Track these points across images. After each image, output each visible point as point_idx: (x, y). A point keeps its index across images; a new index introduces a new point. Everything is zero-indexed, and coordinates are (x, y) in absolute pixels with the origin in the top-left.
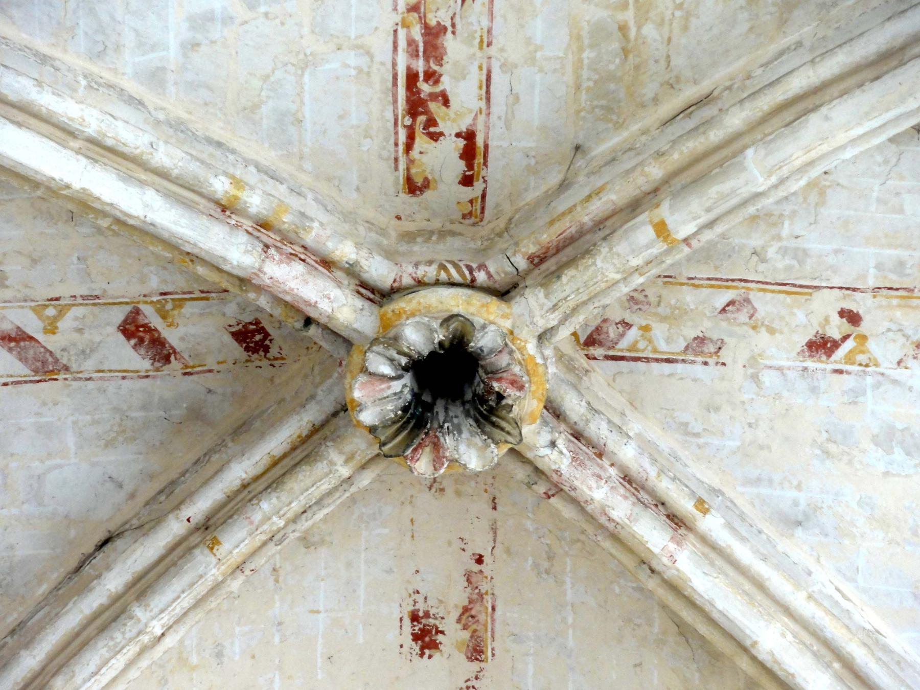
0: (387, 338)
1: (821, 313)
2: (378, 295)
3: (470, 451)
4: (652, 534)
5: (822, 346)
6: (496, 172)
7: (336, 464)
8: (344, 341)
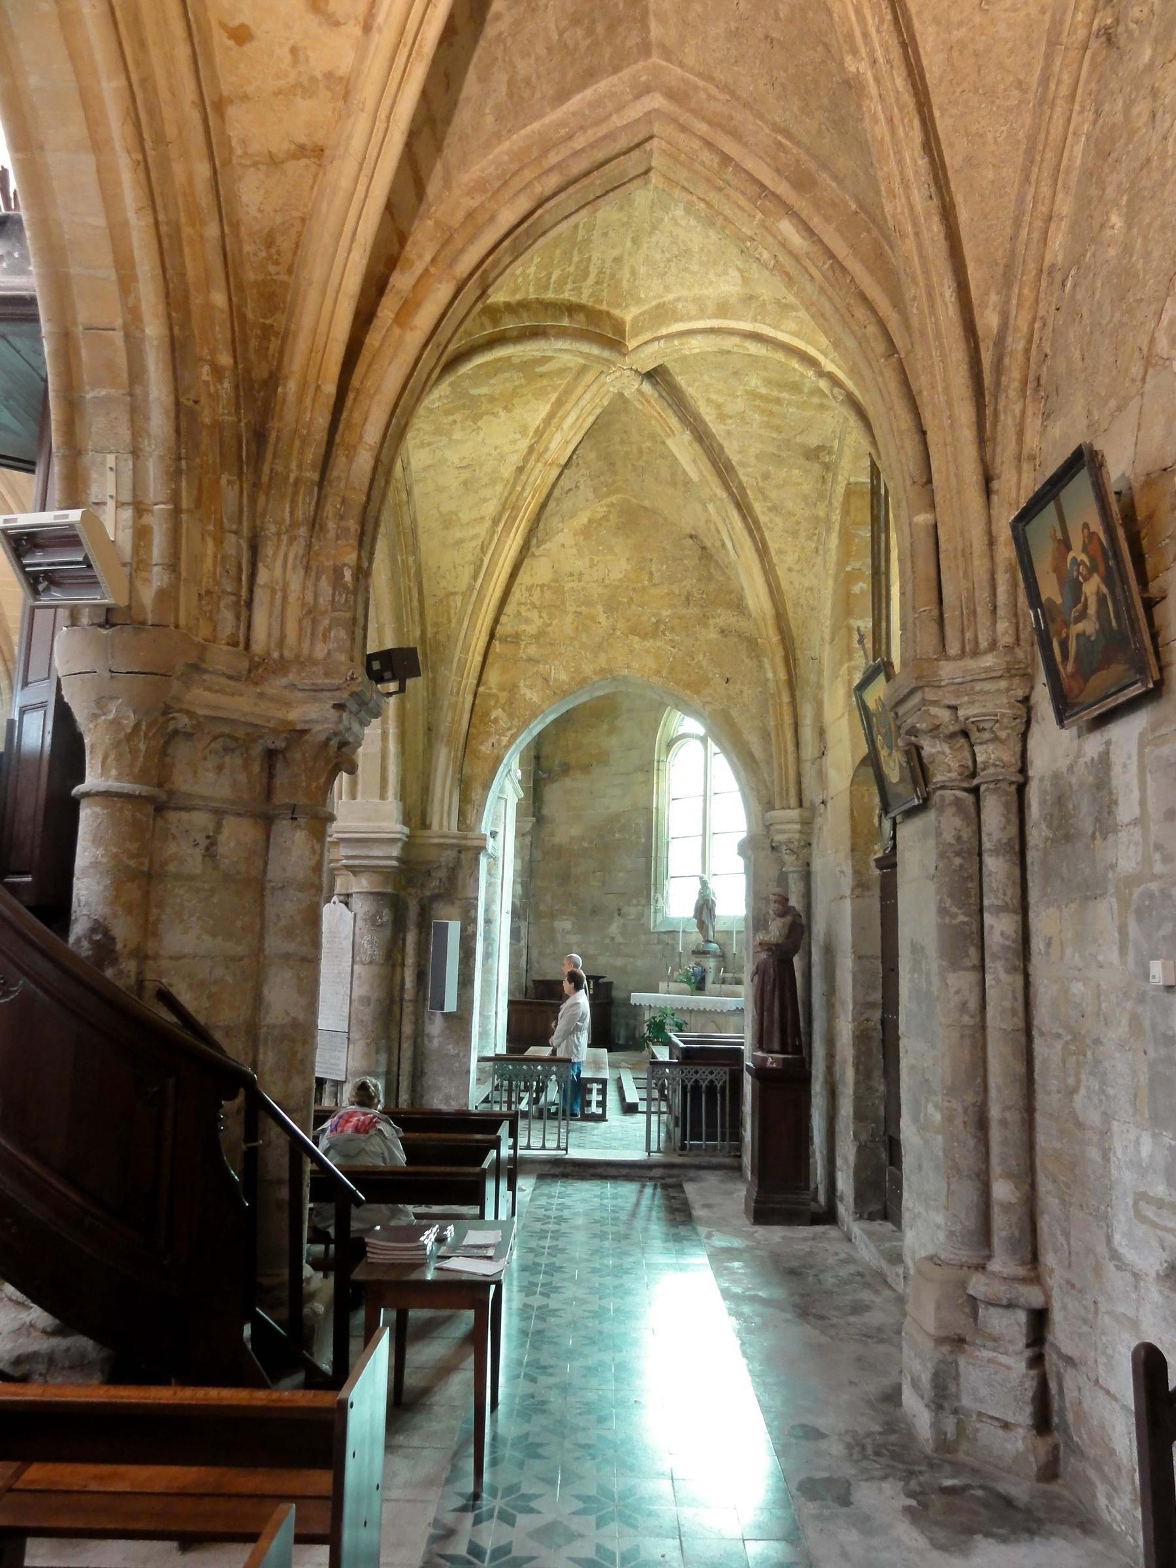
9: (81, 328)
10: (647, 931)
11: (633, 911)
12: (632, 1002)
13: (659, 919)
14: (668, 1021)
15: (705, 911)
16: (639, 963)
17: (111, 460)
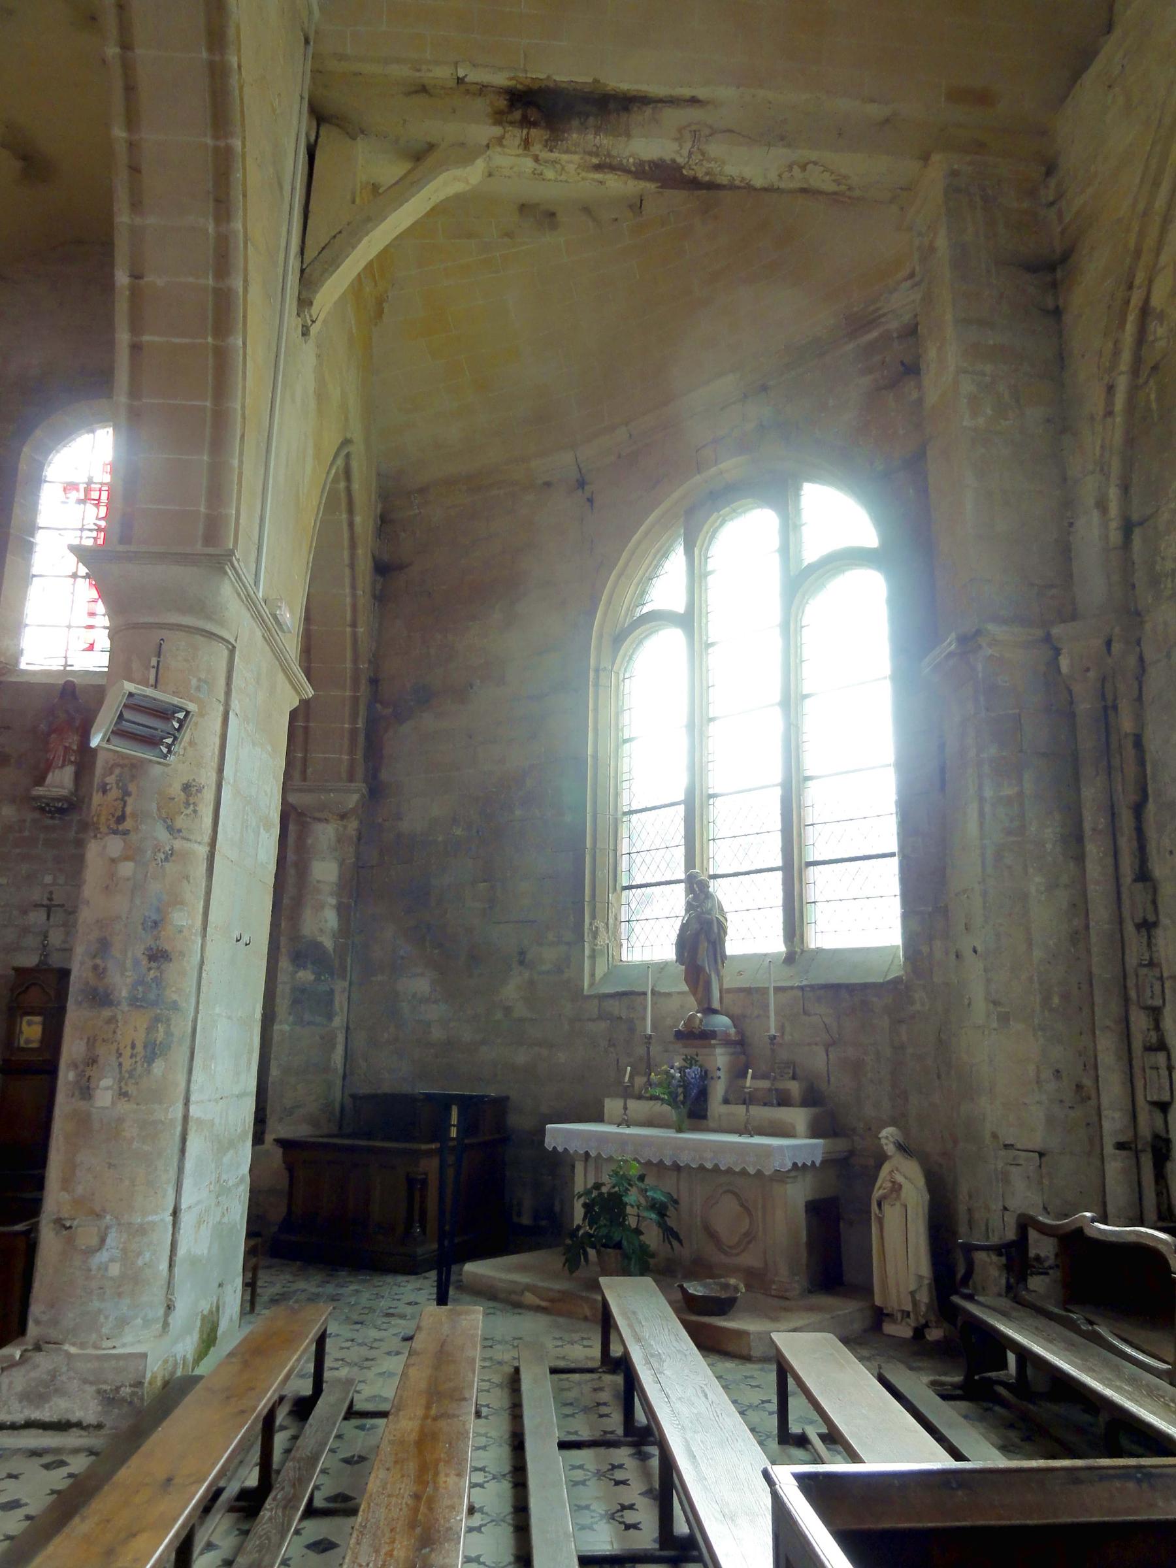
10: (577, 994)
11: (549, 955)
12: (549, 1143)
13: (600, 972)
14: (632, 1197)
15: (704, 945)
16: (562, 1057)
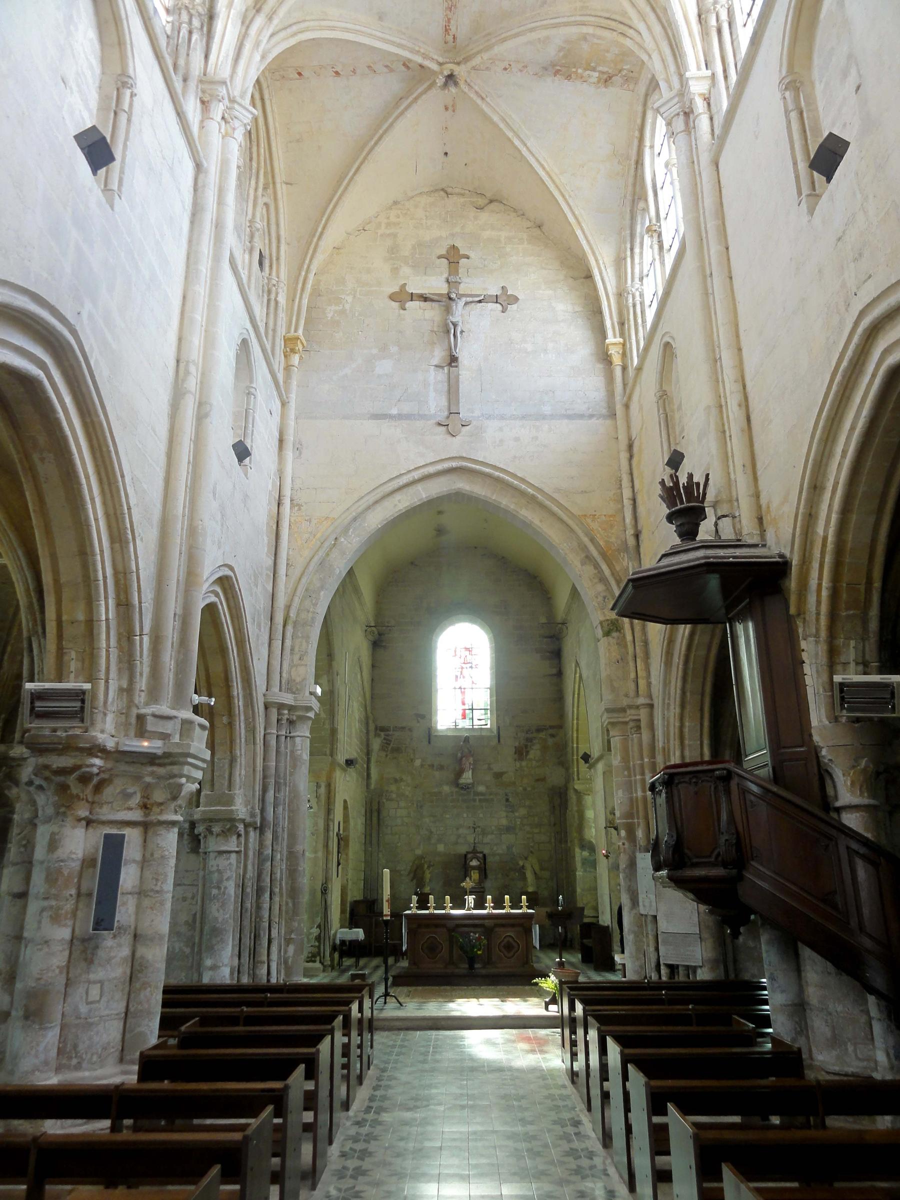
0: (441, 73)
1: (506, 64)
2: (441, 64)
3: (453, 90)
4: (479, 101)
5: (505, 69)
6: (458, 40)
7: (434, 91)
8: (434, 73)
9: (845, 585)
17: (852, 643)
